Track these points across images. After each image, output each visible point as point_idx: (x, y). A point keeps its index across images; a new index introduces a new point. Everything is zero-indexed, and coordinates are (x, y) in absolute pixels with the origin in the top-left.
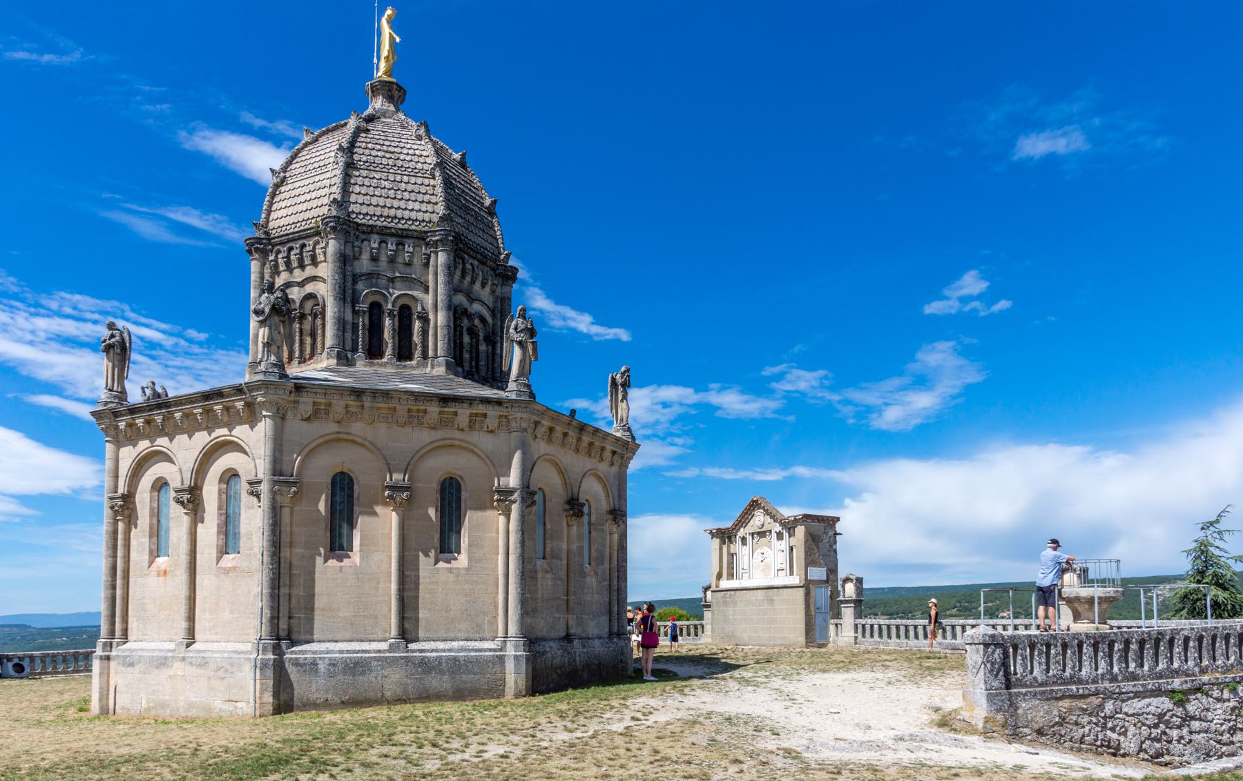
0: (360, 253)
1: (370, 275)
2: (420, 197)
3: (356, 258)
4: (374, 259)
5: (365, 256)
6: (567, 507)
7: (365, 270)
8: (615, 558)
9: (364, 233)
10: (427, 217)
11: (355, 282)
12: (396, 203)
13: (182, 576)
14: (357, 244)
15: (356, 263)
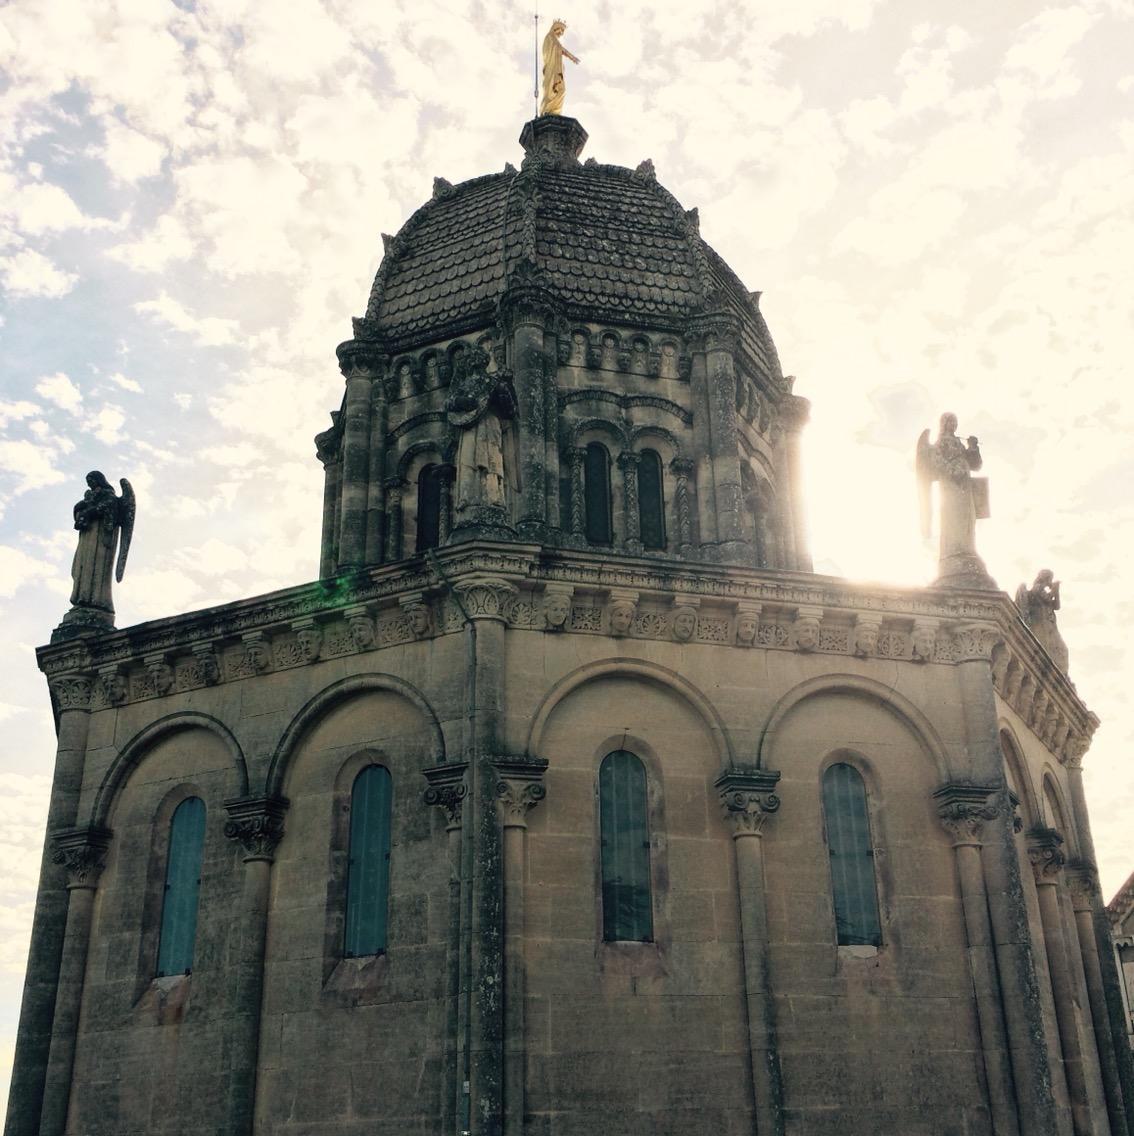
0: (569, 356)
1: (587, 395)
2: (664, 267)
3: (563, 363)
4: (593, 366)
5: (578, 360)
6: (1035, 843)
7: (576, 386)
8: (1096, 967)
9: (574, 319)
10: (679, 296)
11: (561, 406)
12: (625, 276)
13: (223, 1020)
14: (566, 337)
15: (562, 373)
